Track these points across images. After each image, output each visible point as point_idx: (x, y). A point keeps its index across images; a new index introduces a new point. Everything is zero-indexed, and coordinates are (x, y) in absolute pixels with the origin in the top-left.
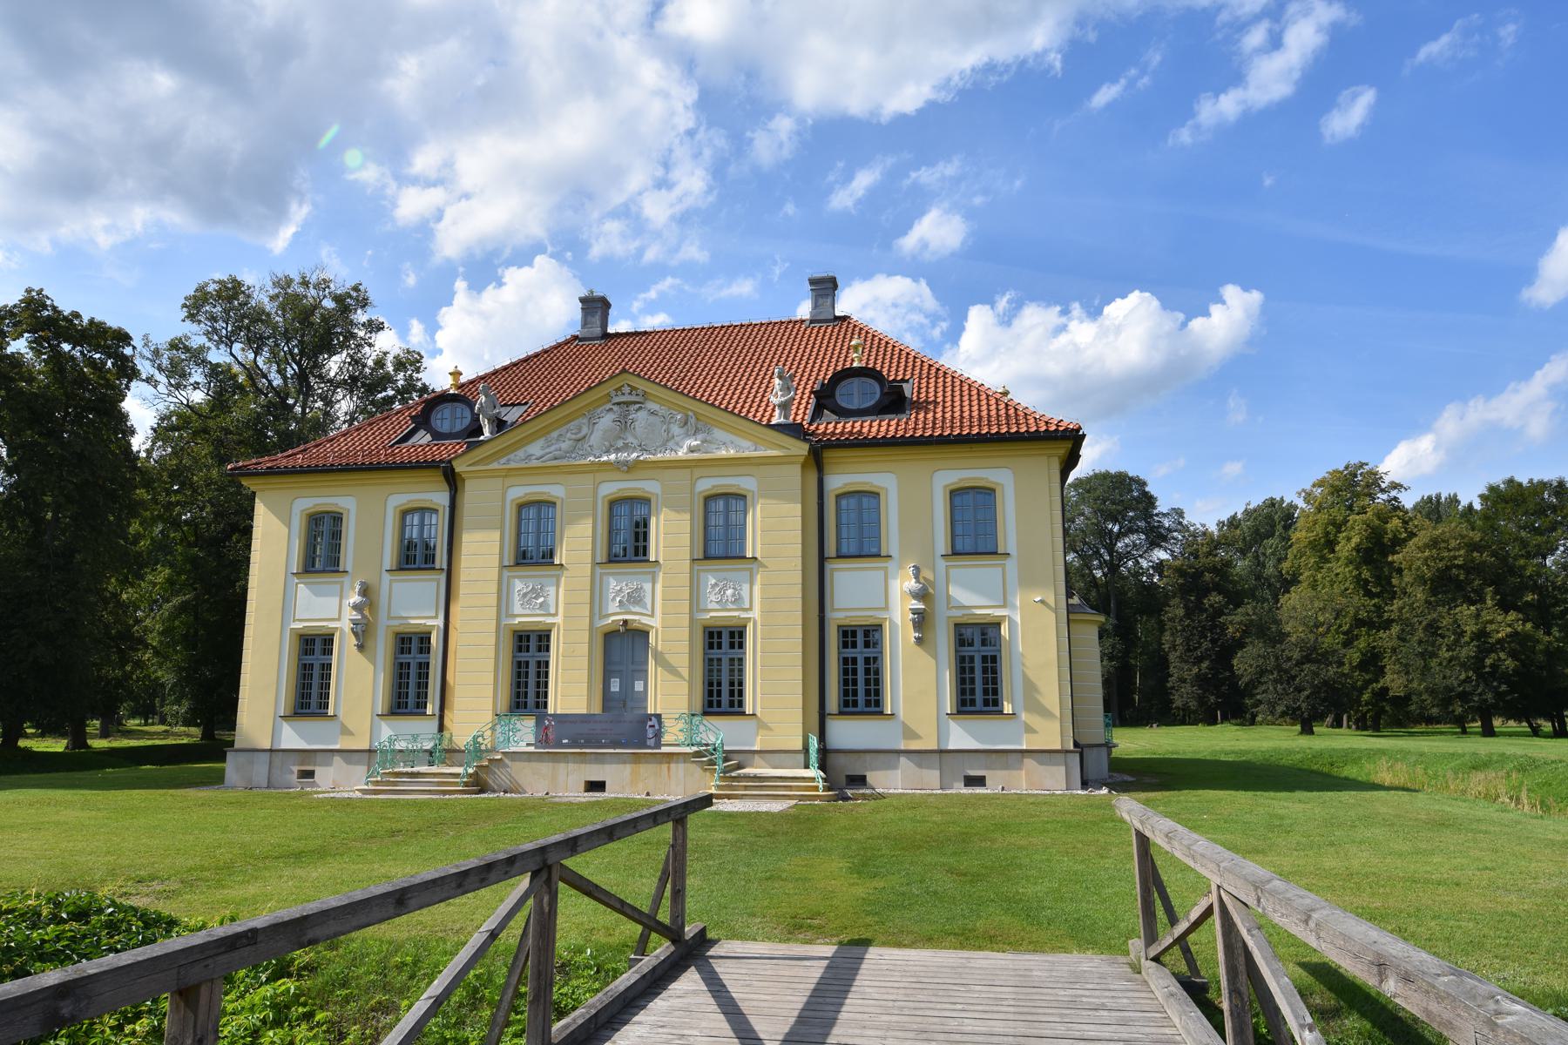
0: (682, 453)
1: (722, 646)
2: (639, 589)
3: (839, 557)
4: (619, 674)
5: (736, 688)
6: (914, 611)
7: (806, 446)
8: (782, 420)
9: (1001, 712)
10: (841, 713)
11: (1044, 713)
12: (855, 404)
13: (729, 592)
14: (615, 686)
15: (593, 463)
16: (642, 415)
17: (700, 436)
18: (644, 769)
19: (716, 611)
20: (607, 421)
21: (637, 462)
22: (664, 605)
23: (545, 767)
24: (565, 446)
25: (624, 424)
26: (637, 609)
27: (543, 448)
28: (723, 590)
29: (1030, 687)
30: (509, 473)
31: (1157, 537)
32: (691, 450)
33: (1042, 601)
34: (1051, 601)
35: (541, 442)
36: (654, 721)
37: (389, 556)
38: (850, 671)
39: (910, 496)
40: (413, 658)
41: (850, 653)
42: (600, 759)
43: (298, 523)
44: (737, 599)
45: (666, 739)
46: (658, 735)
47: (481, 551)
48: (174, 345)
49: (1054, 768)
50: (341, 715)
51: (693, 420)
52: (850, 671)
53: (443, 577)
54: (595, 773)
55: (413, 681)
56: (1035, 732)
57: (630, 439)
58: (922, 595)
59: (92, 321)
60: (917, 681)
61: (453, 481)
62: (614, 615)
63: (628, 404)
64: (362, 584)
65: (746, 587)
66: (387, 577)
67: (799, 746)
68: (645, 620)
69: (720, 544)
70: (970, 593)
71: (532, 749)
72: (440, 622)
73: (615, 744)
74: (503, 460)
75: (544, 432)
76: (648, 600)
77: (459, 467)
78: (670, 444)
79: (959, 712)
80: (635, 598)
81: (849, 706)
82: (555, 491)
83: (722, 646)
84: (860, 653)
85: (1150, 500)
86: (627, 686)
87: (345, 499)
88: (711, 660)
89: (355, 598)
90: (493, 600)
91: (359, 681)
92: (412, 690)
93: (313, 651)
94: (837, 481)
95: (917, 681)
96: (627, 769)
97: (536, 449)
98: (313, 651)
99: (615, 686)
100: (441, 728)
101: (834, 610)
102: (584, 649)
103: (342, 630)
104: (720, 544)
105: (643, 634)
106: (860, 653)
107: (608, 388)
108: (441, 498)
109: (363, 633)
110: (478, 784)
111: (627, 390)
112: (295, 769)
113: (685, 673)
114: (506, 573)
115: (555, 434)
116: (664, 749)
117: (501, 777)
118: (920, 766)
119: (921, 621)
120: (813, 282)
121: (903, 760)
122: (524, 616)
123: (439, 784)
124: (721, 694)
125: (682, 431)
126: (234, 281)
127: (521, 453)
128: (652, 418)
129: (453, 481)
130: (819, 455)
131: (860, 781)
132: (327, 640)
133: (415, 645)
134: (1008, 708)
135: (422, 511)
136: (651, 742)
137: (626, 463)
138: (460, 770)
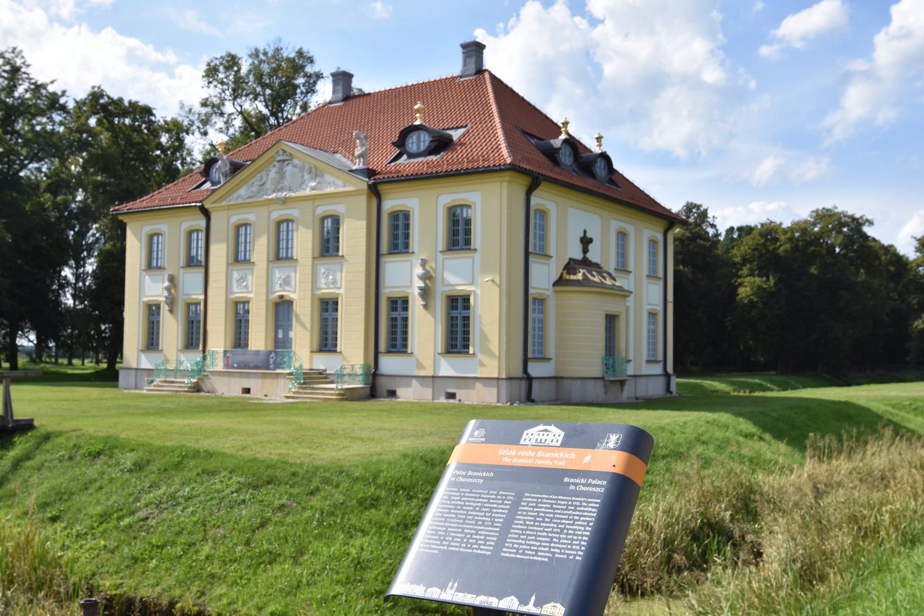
0: (308, 192)
1: (328, 307)
2: (288, 277)
6: (420, 288)
9: (468, 353)
10: (389, 352)
11: (490, 354)
13: (331, 277)
14: (280, 335)
15: (266, 200)
16: (290, 167)
18: (268, 381)
19: (325, 290)
20: (273, 173)
23: (225, 379)
24: (254, 189)
25: (281, 175)
26: (287, 288)
28: (327, 276)
29: (484, 338)
30: (230, 207)
32: (313, 189)
33: (493, 281)
34: (497, 280)
35: (245, 188)
37: (182, 261)
41: (394, 314)
42: (248, 375)
43: (144, 239)
44: (334, 282)
47: (219, 253)
48: (204, 104)
49: (491, 389)
54: (246, 383)
55: (460, 329)
56: (485, 366)
59: (130, 102)
60: (426, 328)
61: (206, 213)
63: (284, 161)
64: (169, 275)
65: (339, 274)
66: (182, 271)
69: (328, 246)
70: (456, 275)
72: (202, 297)
73: (256, 367)
76: (293, 283)
77: (207, 206)
78: (303, 186)
79: (449, 352)
80: (286, 282)
82: (251, 217)
84: (398, 314)
86: (286, 334)
88: (452, 318)
89: (167, 284)
90: (223, 284)
91: (172, 329)
92: (459, 336)
94: (391, 204)
95: (426, 328)
96: (259, 381)
97: (243, 192)
102: (263, 312)
104: (328, 246)
106: (398, 314)
107: (272, 153)
108: (202, 223)
110: (197, 388)
111: (281, 152)
112: (146, 379)
113: (309, 326)
114: (271, 265)
117: (206, 385)
118: (422, 385)
119: (425, 293)
120: (464, 46)
121: (414, 382)
122: (238, 293)
124: (327, 342)
126: (230, 55)
127: (235, 195)
129: (206, 213)
131: (392, 394)
132: (158, 306)
133: (460, 304)
134: (471, 351)
135: (198, 231)
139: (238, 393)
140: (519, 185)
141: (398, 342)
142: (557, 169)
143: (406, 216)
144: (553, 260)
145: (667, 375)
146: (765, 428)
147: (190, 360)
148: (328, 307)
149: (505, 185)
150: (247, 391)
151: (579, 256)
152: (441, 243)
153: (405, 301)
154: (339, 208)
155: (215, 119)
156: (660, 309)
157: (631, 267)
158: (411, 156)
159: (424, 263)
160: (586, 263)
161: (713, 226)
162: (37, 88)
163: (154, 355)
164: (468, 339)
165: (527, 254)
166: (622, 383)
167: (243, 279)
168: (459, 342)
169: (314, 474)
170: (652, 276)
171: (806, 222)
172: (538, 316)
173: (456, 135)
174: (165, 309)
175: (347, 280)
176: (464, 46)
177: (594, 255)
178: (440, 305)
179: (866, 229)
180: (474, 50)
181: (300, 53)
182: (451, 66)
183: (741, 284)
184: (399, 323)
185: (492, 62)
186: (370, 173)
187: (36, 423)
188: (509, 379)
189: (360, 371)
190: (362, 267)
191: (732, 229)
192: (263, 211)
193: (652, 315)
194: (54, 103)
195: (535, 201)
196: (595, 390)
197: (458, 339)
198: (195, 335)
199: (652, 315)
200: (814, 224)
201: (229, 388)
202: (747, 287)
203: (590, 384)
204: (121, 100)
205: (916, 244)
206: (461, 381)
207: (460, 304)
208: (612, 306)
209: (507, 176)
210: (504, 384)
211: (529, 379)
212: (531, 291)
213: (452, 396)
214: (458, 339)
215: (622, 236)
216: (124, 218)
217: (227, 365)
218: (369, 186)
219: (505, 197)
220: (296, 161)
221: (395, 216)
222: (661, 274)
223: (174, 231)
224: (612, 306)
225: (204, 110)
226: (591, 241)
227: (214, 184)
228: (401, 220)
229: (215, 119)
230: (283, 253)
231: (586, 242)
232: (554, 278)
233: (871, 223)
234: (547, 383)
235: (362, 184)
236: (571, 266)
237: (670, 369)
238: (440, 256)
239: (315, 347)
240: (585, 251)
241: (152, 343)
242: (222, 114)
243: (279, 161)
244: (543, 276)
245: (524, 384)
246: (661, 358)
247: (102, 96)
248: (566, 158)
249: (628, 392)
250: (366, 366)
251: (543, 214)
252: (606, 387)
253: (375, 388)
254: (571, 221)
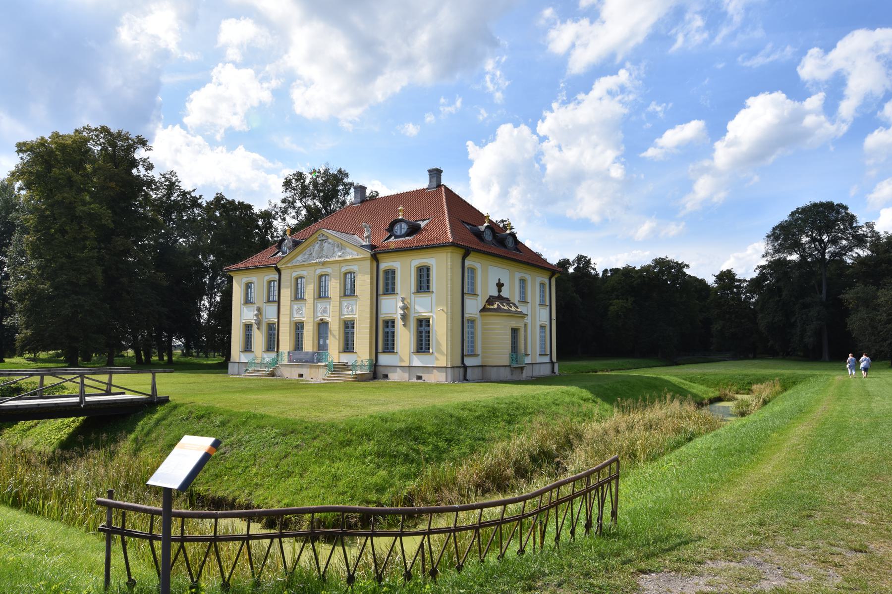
0: (337, 259)
1: (348, 326)
18: (313, 370)
19: (347, 316)
23: (289, 369)
25: (322, 248)
29: (438, 343)
30: (292, 267)
31: (860, 241)
38: (384, 338)
39: (405, 268)
41: (387, 330)
42: (302, 366)
44: (352, 311)
47: (286, 294)
48: (284, 201)
52: (384, 338)
54: (301, 371)
58: (405, 308)
60: (405, 338)
61: (279, 271)
62: (320, 316)
69: (349, 292)
70: (422, 306)
73: (306, 362)
85: (852, 218)
91: (259, 339)
94: (384, 265)
95: (405, 338)
97: (299, 258)
102: (311, 328)
104: (349, 292)
107: (316, 235)
108: (276, 276)
110: (272, 374)
117: (278, 372)
119: (404, 317)
120: (429, 171)
121: (398, 369)
122: (297, 318)
124: (348, 346)
129: (279, 271)
130: (375, 258)
131: (386, 376)
135: (274, 281)
139: (296, 377)
140: (458, 255)
141: (389, 346)
142: (482, 244)
143: (394, 272)
144: (479, 298)
145: (552, 363)
146: (598, 396)
147: (269, 357)
148: (348, 326)
149: (449, 254)
150: (301, 375)
151: (496, 294)
152: (413, 288)
153: (393, 322)
154: (355, 268)
155: (290, 210)
156: (548, 323)
157: (529, 300)
158: (396, 237)
159: (403, 300)
160: (500, 298)
161: (594, 269)
162: (184, 194)
163: (248, 354)
164: (429, 344)
165: (463, 294)
166: (522, 368)
167: (299, 309)
168: (424, 346)
169: (317, 427)
170: (542, 304)
171: (650, 266)
172: (470, 330)
173: (423, 224)
174: (255, 327)
175: (359, 310)
176: (429, 171)
177: (505, 293)
178: (413, 324)
179: (685, 270)
180: (436, 173)
181: (340, 171)
182: (422, 183)
183: (611, 304)
184: (390, 335)
185: (446, 181)
186: (372, 247)
187: (170, 399)
188: (453, 367)
189: (367, 364)
190: (368, 302)
191: (606, 270)
192: (311, 269)
193: (543, 327)
194: (195, 202)
195: (467, 263)
196: (505, 374)
197: (423, 344)
198: (272, 344)
199: (543, 327)
200: (655, 267)
201: (291, 374)
202: (616, 305)
203: (502, 370)
204: (233, 201)
205: (714, 279)
207: (424, 323)
208: (516, 323)
209: (450, 249)
210: (449, 370)
211: (465, 367)
212: (466, 315)
213: (420, 378)
214: (423, 344)
215: (523, 281)
216: (232, 274)
217: (290, 361)
218: (372, 255)
219: (449, 261)
220: (330, 240)
221: (387, 272)
222: (548, 303)
223: (260, 280)
224: (516, 323)
225: (283, 205)
226: (503, 285)
227: (283, 253)
228: (390, 274)
229: (290, 210)
230: (323, 294)
231: (500, 286)
232: (481, 307)
233: (688, 266)
234: (476, 369)
235: (368, 254)
236: (491, 300)
237: (554, 359)
238: (413, 296)
240: (500, 291)
241: (248, 347)
242: (294, 208)
244: (473, 306)
245: (462, 370)
246: (548, 352)
247: (222, 199)
248: (488, 237)
249: (526, 374)
250: (370, 361)
251: (473, 270)
252: (512, 371)
253: (375, 373)
254: (490, 275)
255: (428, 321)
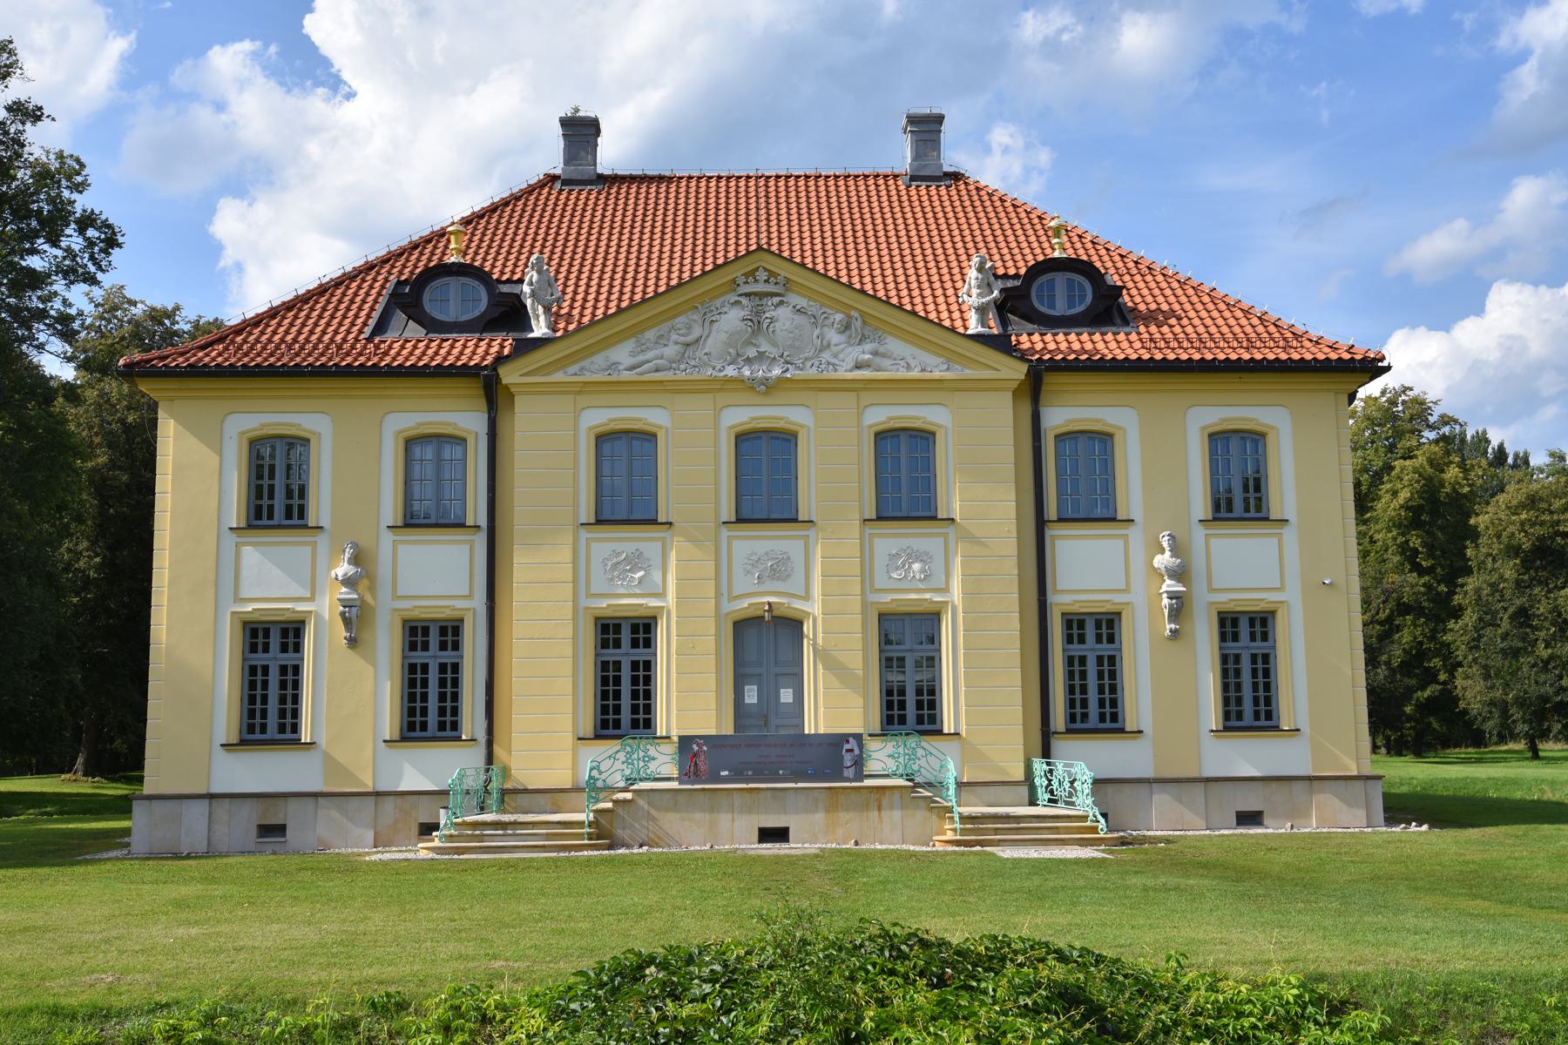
3: (1060, 520)
4: (757, 678)
5: (1078, 696)
7: (1024, 368)
8: (980, 329)
10: (1069, 731)
12: (1061, 308)
14: (751, 696)
16: (783, 313)
17: (868, 347)
20: (732, 319)
21: (780, 380)
22: (830, 583)
24: (671, 351)
25: (756, 324)
27: (633, 354)
35: (630, 345)
36: (853, 744)
40: (433, 657)
45: (872, 766)
46: (859, 763)
50: (323, 741)
51: (859, 324)
53: (481, 540)
57: (765, 347)
60: (1169, 683)
62: (753, 598)
66: (387, 538)
67: (1019, 775)
68: (798, 605)
71: (674, 785)
74: (572, 370)
75: (635, 331)
79: (1226, 729)
81: (1078, 724)
82: (652, 416)
83: (1246, 640)
84: (1091, 649)
87: (312, 418)
89: (343, 569)
93: (271, 651)
94: (1057, 417)
95: (1169, 683)
97: (622, 354)
98: (271, 651)
99: (751, 696)
100: (490, 759)
101: (1056, 591)
102: (710, 643)
103: (318, 617)
105: (794, 625)
106: (1091, 649)
107: (737, 272)
108: (469, 420)
109: (355, 619)
111: (762, 275)
115: (650, 335)
116: (868, 782)
123: (548, 837)
125: (842, 338)
127: (599, 360)
128: (799, 319)
130: (1039, 378)
136: (849, 773)
137: (765, 381)
138: (581, 817)
150: (776, 835)
175: (966, 577)
180: (926, 128)
197: (1250, 700)
206: (1274, 785)
214: (1250, 700)
239: (588, 727)
243: (748, 295)
255: (1262, 623)
